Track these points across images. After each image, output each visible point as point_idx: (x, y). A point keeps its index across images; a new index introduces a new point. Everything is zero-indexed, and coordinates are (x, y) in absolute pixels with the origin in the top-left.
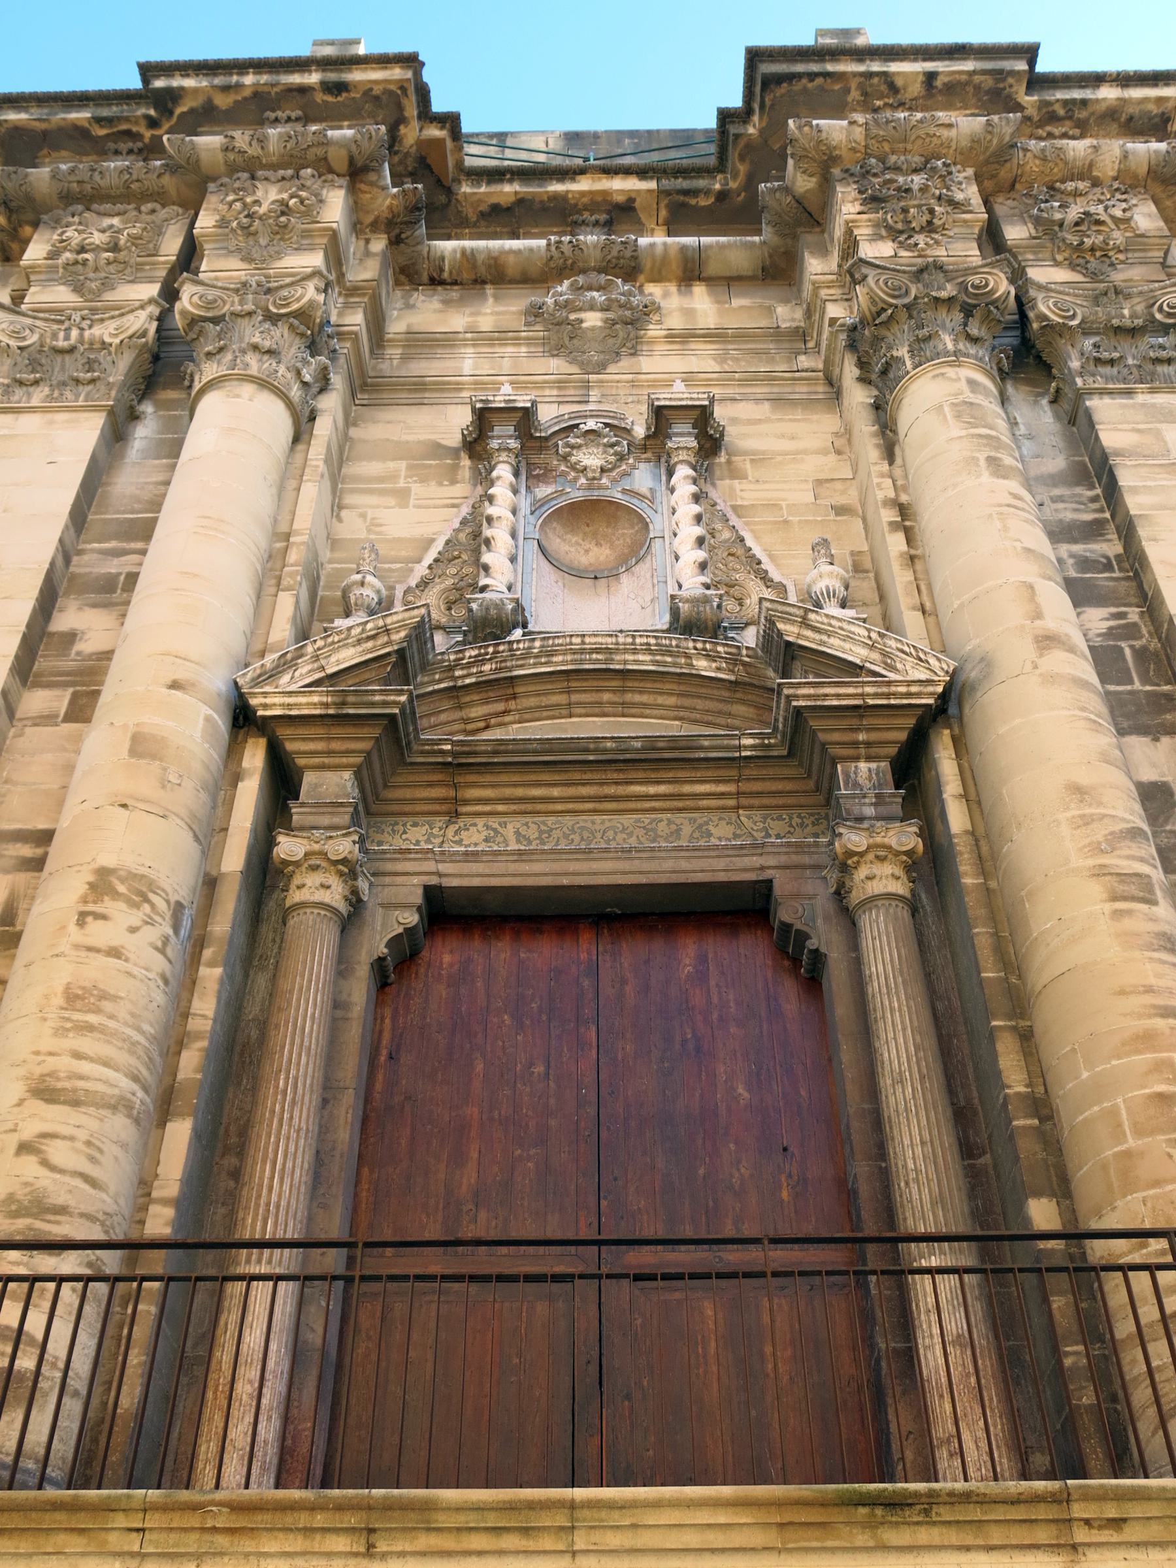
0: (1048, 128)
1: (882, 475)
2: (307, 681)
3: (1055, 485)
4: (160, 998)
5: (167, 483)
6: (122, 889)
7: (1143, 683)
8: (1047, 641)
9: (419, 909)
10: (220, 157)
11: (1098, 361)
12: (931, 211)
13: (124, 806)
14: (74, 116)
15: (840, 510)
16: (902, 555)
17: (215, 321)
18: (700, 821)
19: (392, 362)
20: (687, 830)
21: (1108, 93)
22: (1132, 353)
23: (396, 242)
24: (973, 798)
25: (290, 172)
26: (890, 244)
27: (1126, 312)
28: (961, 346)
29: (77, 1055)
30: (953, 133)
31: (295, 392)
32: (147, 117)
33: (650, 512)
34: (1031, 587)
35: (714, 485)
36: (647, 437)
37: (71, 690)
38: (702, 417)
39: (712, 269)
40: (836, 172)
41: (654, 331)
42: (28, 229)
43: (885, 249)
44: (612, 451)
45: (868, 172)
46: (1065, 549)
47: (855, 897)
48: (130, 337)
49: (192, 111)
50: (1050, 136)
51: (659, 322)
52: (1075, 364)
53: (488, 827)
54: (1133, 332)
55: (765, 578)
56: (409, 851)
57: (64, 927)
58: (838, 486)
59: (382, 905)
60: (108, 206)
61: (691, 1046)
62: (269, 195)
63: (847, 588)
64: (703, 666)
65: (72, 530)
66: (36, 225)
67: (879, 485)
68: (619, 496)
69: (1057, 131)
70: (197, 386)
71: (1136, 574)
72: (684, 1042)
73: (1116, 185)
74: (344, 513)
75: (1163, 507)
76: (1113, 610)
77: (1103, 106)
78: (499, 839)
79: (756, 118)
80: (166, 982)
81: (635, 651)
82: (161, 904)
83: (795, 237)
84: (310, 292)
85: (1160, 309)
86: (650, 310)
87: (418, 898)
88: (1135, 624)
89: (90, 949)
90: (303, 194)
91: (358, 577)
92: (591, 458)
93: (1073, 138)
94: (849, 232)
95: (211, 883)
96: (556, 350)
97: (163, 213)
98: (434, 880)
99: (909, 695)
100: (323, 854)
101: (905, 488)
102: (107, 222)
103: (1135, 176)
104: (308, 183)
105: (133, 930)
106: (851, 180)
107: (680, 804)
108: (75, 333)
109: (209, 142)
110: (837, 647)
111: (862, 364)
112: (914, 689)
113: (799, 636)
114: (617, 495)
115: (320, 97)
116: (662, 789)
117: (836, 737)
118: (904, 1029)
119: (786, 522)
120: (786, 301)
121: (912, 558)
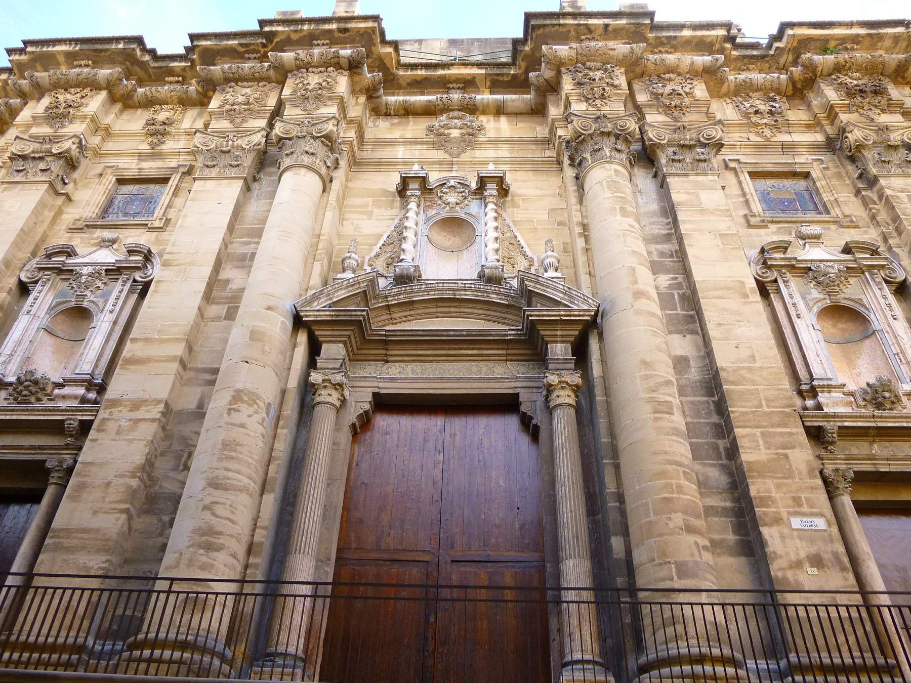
0: (659, 48)
1: (576, 211)
2: (325, 305)
3: (652, 217)
5: (269, 211)
6: (246, 398)
7: (682, 310)
8: (638, 294)
9: (370, 402)
10: (294, 61)
11: (673, 160)
12: (604, 89)
13: (247, 362)
14: (230, 42)
15: (560, 224)
16: (582, 249)
17: (290, 139)
18: (490, 366)
19: (368, 153)
20: (484, 370)
21: (687, 33)
22: (688, 157)
23: (370, 98)
24: (603, 361)
25: (323, 69)
26: (585, 104)
27: (688, 137)
28: (613, 154)
30: (615, 53)
31: (324, 171)
32: (262, 43)
33: (476, 223)
34: (634, 269)
35: (505, 210)
36: (477, 189)
37: (227, 306)
38: (500, 180)
39: (509, 109)
40: (563, 70)
41: (482, 138)
42: (211, 93)
43: (583, 106)
44: (461, 195)
45: (577, 71)
46: (653, 247)
47: (552, 404)
48: (254, 146)
49: (281, 40)
50: (660, 52)
51: (484, 134)
52: (663, 161)
53: (400, 367)
54: (690, 147)
55: (525, 255)
56: (366, 377)
57: (221, 415)
58: (559, 212)
59: (355, 401)
60: (245, 83)
61: (482, 463)
62: (314, 80)
63: (558, 262)
64: (494, 298)
65: (228, 234)
66: (214, 91)
67: (575, 215)
68: (463, 215)
69: (663, 50)
70: (282, 169)
71: (683, 260)
72: (479, 461)
73: (688, 76)
74: (344, 222)
75: (696, 230)
76: (672, 276)
77: (684, 39)
78: (405, 372)
79: (529, 42)
80: (263, 437)
81: (465, 290)
83: (545, 97)
84: (330, 127)
85: (703, 136)
86: (481, 128)
87: (370, 397)
88: (681, 283)
89: (232, 424)
90: (329, 80)
91: (349, 255)
92: (452, 198)
93: (671, 53)
94: (567, 98)
95: (284, 392)
96: (440, 146)
97: (269, 86)
98: (377, 390)
99: (579, 316)
100: (329, 381)
101: (586, 217)
102: (244, 91)
103: (697, 72)
104: (331, 74)
105: (250, 416)
106: (570, 73)
107: (482, 358)
108: (230, 143)
109: (288, 56)
110: (550, 293)
111: (572, 159)
112: (581, 313)
113: (535, 287)
114: (463, 216)
115: (337, 35)
116: (474, 352)
117: (548, 333)
118: (567, 463)
119: (535, 228)
120: (542, 125)
121: (587, 250)
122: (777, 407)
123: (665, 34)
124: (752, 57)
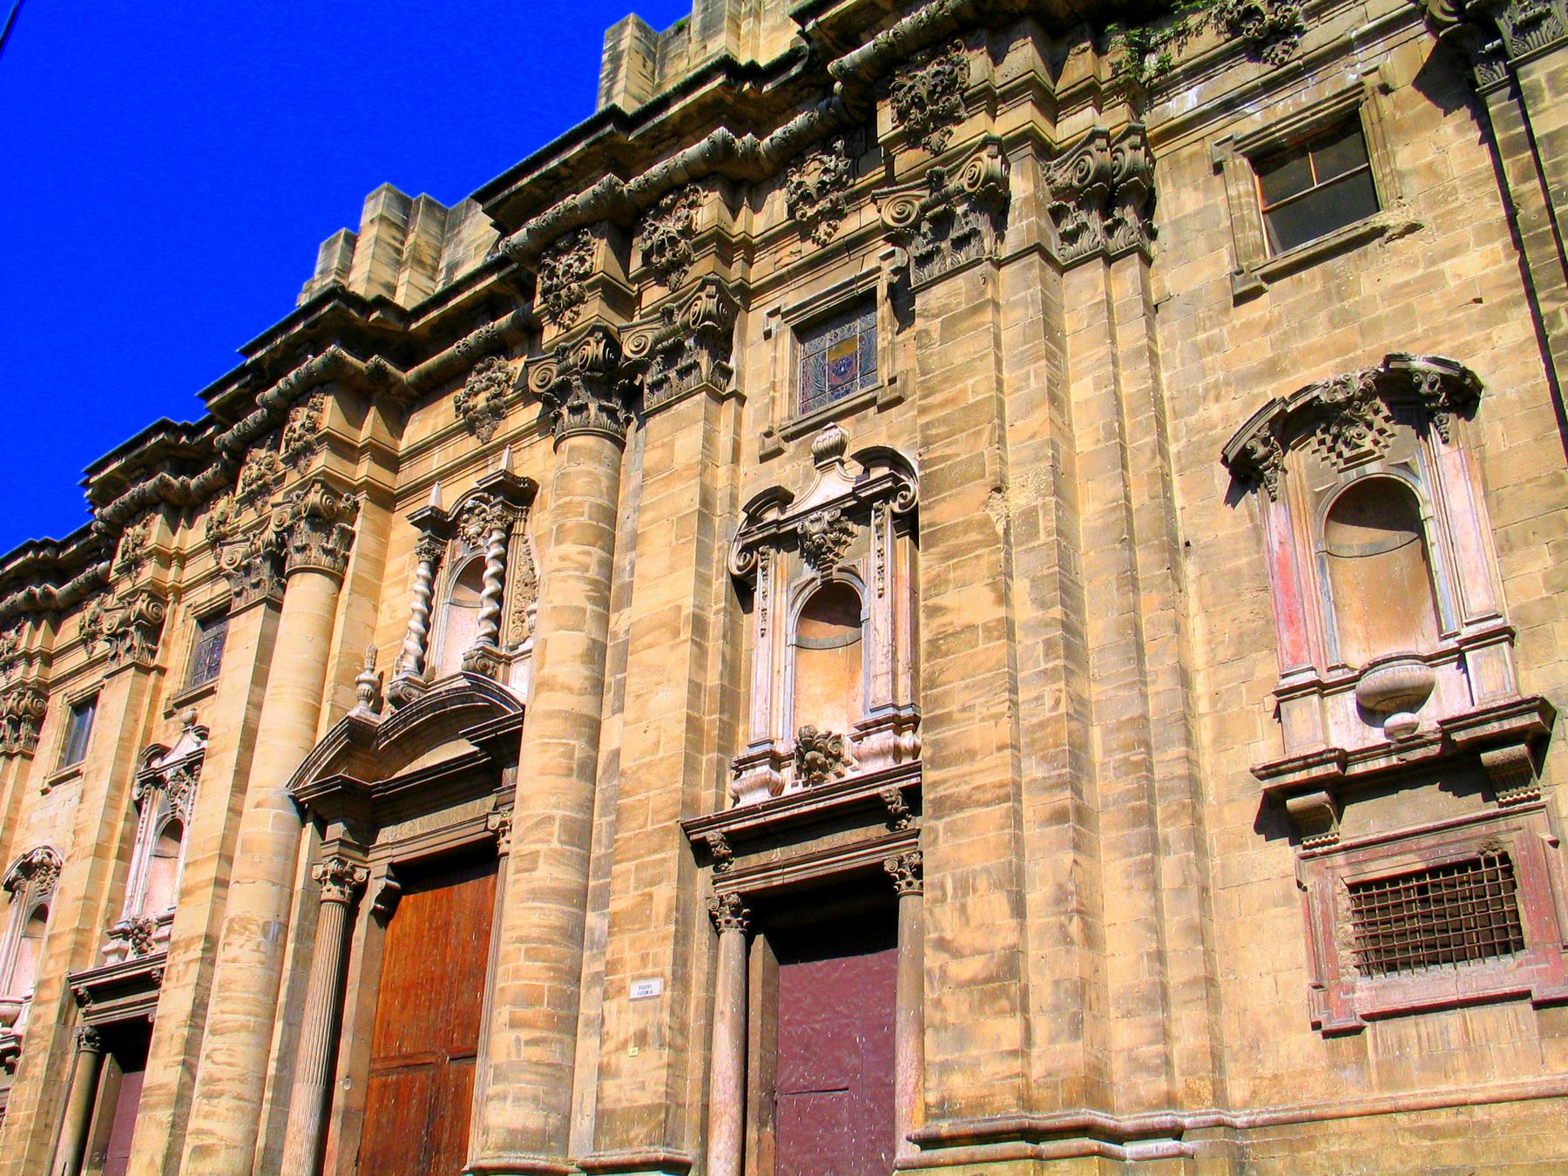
4: (259, 971)
29: (223, 1013)
31: (326, 561)
80: (263, 963)
82: (253, 928)
98: (390, 860)
105: (241, 947)
122: (661, 822)
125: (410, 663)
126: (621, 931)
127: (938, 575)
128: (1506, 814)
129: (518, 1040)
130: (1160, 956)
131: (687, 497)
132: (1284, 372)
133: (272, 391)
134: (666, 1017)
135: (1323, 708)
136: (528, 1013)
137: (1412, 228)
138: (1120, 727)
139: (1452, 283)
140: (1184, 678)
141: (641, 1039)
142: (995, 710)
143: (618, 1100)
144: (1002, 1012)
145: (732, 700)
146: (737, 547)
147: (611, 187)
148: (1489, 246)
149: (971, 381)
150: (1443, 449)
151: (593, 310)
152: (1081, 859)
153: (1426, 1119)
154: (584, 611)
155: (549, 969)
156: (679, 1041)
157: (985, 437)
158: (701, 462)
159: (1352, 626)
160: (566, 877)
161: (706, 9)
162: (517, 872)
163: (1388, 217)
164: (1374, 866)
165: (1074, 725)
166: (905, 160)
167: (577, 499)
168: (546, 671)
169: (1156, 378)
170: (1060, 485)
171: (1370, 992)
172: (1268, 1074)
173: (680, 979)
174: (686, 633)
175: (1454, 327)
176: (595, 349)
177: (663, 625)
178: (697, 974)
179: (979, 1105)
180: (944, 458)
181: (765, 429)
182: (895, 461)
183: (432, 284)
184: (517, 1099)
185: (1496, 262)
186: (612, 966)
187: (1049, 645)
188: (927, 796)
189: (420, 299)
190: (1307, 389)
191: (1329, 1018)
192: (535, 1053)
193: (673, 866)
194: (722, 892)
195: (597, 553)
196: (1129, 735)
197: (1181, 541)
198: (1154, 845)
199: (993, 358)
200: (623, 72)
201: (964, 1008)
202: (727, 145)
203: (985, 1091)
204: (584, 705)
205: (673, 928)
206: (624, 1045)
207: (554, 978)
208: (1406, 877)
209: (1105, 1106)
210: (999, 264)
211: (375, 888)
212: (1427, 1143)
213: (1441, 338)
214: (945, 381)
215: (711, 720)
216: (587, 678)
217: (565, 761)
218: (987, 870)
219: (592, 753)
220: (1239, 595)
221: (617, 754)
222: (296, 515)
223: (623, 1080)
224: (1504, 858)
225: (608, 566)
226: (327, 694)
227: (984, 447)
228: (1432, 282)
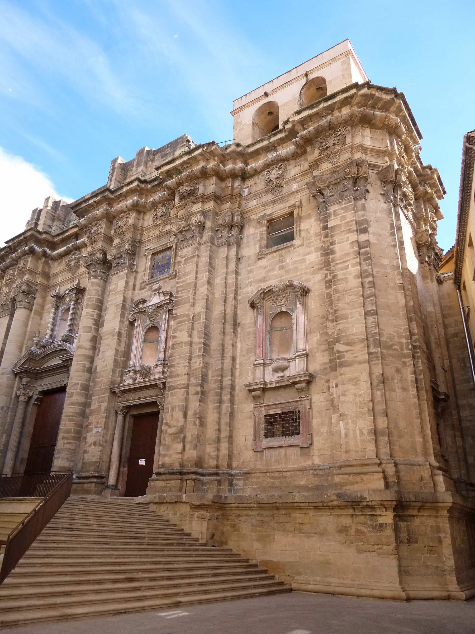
31: (26, 305)
123: (117, 194)
124: (156, 185)
125: (47, 337)
126: (93, 415)
127: (176, 328)
128: (300, 401)
129: (64, 443)
130: (219, 430)
131: (119, 299)
132: (267, 281)
133: (13, 255)
134: (101, 438)
135: (264, 370)
136: (66, 435)
137: (302, 245)
138: (216, 370)
139: (308, 262)
140: (234, 359)
141: (95, 444)
142: (185, 365)
143: (88, 460)
144: (178, 442)
145: (127, 354)
146: (131, 314)
147: (107, 209)
148: (317, 253)
149: (189, 277)
150: (299, 306)
151: (100, 244)
152: (201, 404)
153: (273, 475)
154: (91, 327)
155: (74, 424)
156: (105, 444)
157: (191, 292)
158: (124, 290)
159: (275, 349)
160: (82, 399)
161: (138, 158)
162: (68, 397)
163: (296, 242)
164: (271, 411)
165: (204, 370)
166: (181, 213)
167: (92, 296)
168: (80, 343)
169: (237, 279)
170: (208, 307)
171: (265, 442)
172: (242, 461)
173: (106, 427)
174: (116, 336)
175: (306, 273)
176: (100, 256)
177: (111, 333)
178: (111, 427)
179: (171, 465)
180: (181, 297)
181: (141, 281)
182: (171, 295)
183: (63, 226)
184: (62, 458)
185: (318, 258)
186: (90, 424)
187: (200, 348)
188: (167, 385)
189: (59, 231)
190: (270, 286)
191: (256, 449)
192: (68, 446)
193: (107, 398)
194: (119, 406)
195: (97, 311)
196: (218, 373)
197: (238, 322)
198: (221, 401)
199: (195, 271)
200: (115, 174)
201: (170, 440)
202: (137, 202)
203: (173, 462)
204: (90, 353)
205: (105, 414)
206: (90, 445)
207: (75, 426)
208: (277, 414)
209: (201, 467)
210: (200, 244)
211: (35, 397)
212: (272, 480)
213: (303, 276)
214: (184, 275)
215: (121, 359)
216: (91, 346)
217: (83, 368)
218: (178, 406)
219: (91, 365)
220: (249, 338)
221: (96, 366)
222: (19, 292)
223: (89, 454)
224: (299, 411)
225: (100, 316)
226: (25, 343)
227: (191, 295)
228: (304, 260)
